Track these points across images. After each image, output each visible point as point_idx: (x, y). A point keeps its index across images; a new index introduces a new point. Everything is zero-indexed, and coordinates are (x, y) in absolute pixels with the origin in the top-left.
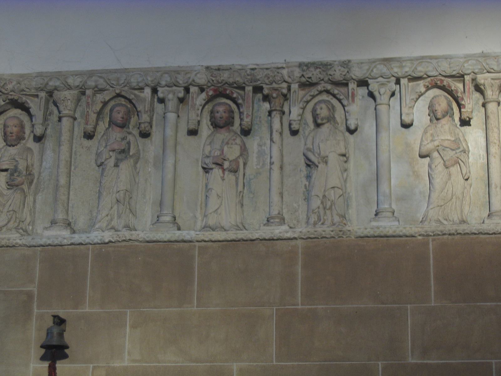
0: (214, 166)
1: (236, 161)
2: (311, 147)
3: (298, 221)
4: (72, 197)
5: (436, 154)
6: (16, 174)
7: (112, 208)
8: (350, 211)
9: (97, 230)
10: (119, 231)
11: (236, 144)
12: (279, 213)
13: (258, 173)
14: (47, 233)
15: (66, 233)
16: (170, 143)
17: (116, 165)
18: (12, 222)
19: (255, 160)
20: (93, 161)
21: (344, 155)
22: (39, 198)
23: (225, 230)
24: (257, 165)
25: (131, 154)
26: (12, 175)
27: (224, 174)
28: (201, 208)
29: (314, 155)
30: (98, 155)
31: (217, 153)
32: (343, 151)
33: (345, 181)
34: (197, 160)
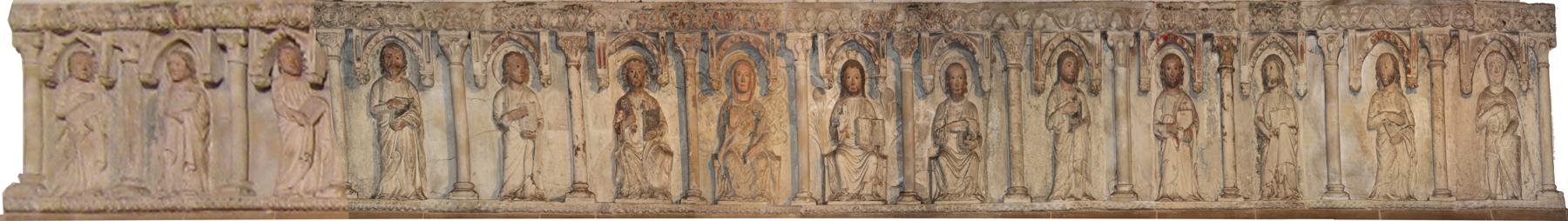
0: (1168, 135)
1: (1189, 129)
2: (1262, 115)
3: (1252, 193)
4: (1026, 163)
5: (1382, 129)
6: (968, 138)
7: (1069, 177)
8: (1301, 184)
9: (1057, 198)
10: (1080, 200)
11: (1187, 109)
12: (1234, 187)
13: (1209, 143)
14: (1007, 200)
15: (1027, 201)
16: (1122, 108)
17: (1071, 131)
18: (969, 189)
19: (1206, 127)
20: (1043, 126)
21: (1292, 127)
22: (990, 162)
23: (1184, 200)
24: (1208, 133)
25: (1083, 117)
26: (965, 138)
27: (1178, 144)
28: (1156, 177)
29: (1265, 126)
30: (1049, 117)
31: (1169, 120)
32: (1294, 124)
33: (1296, 155)
34: (1149, 126)
